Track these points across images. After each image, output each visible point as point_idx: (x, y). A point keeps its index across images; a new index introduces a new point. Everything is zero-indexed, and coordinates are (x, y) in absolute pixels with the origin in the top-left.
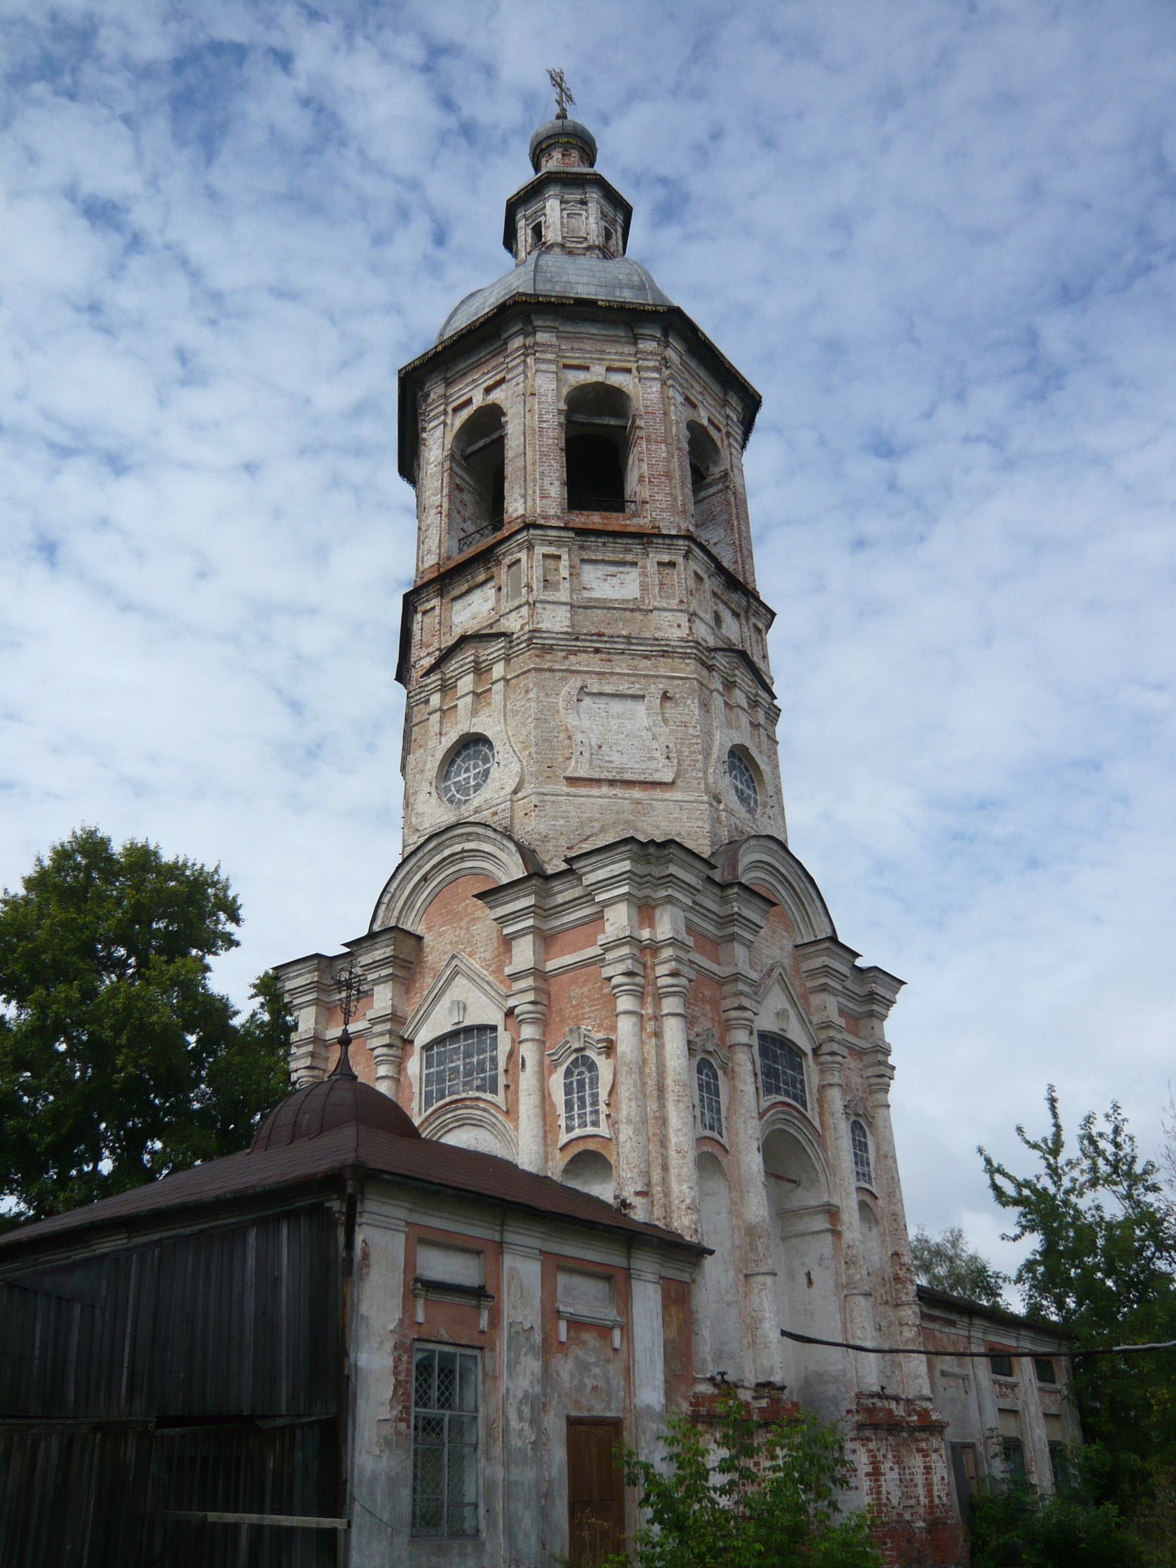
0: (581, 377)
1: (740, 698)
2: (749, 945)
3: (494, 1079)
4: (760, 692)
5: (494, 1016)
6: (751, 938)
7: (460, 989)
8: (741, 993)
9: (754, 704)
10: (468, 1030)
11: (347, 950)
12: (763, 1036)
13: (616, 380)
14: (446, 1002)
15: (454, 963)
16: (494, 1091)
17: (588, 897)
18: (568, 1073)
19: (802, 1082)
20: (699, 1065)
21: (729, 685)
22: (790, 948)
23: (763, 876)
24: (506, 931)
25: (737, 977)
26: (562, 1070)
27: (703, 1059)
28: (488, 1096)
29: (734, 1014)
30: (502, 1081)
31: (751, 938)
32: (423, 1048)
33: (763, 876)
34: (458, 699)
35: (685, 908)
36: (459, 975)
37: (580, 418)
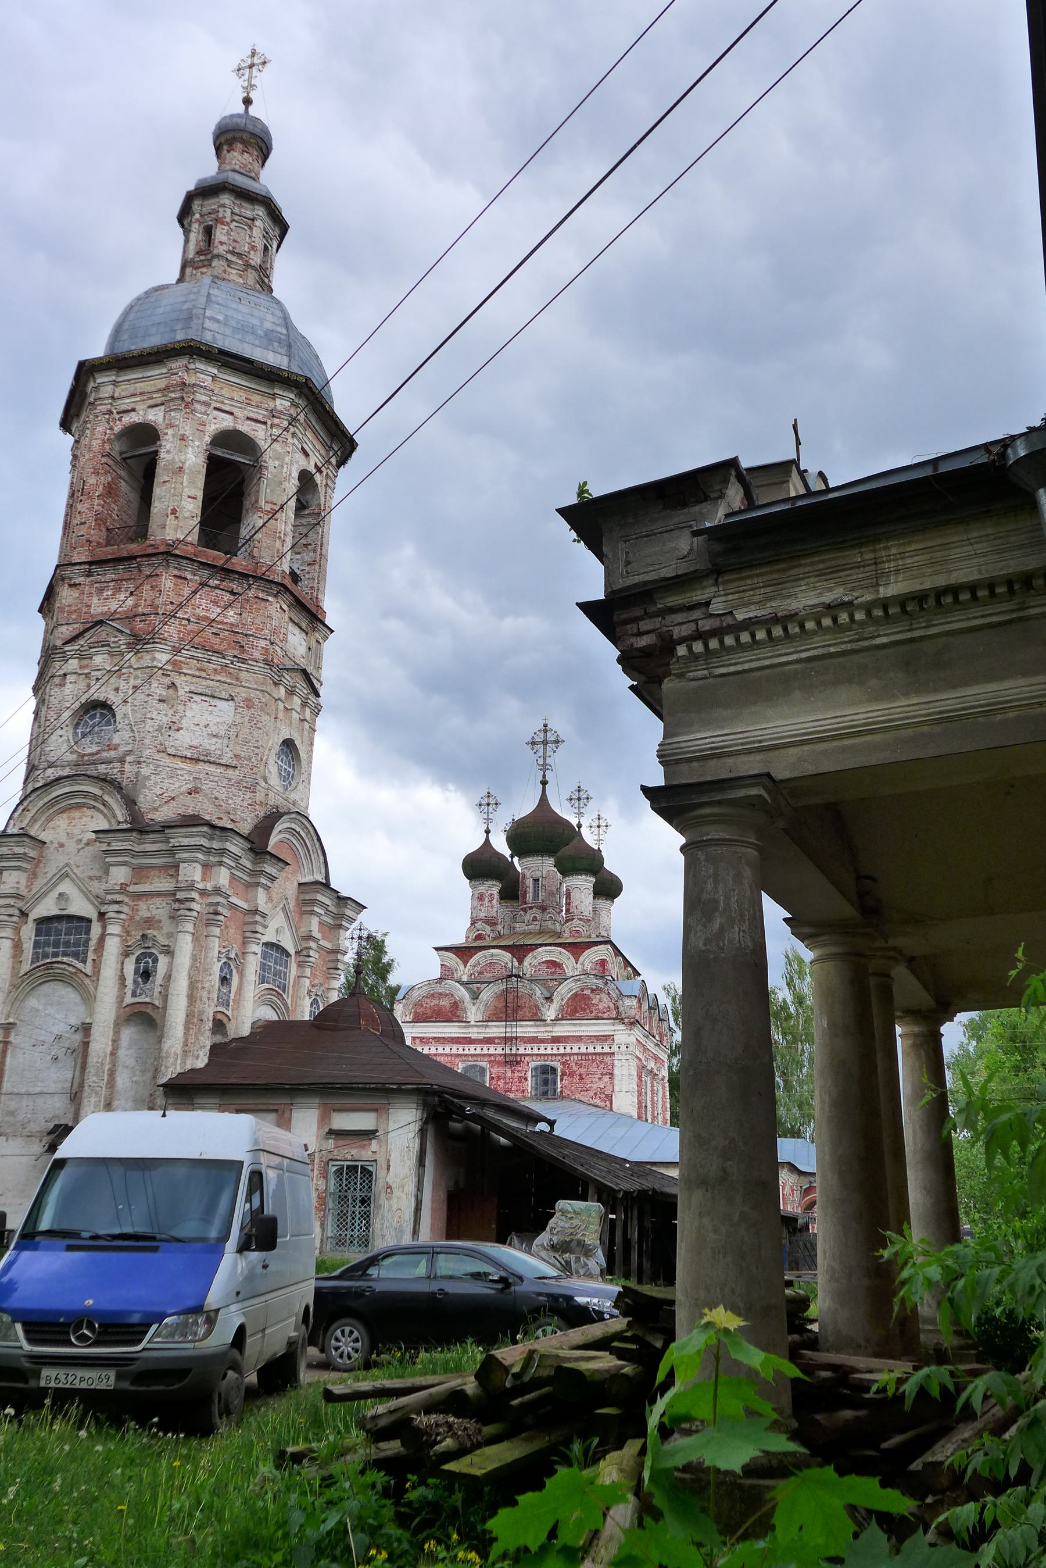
1: (297, 701)
2: (267, 888)
3: (85, 953)
5: (93, 914)
6: (269, 884)
7: (66, 887)
8: (256, 923)
9: (304, 704)
10: (70, 918)
12: (267, 944)
14: (54, 894)
15: (66, 869)
16: (84, 962)
17: (172, 852)
19: (285, 973)
21: (291, 692)
22: (296, 884)
23: (287, 836)
24: (107, 860)
25: (255, 912)
26: (133, 958)
27: (225, 963)
29: (248, 934)
30: (91, 956)
31: (269, 884)
32: (35, 920)
33: (287, 836)
35: (230, 868)
36: (67, 879)
37: (219, 452)
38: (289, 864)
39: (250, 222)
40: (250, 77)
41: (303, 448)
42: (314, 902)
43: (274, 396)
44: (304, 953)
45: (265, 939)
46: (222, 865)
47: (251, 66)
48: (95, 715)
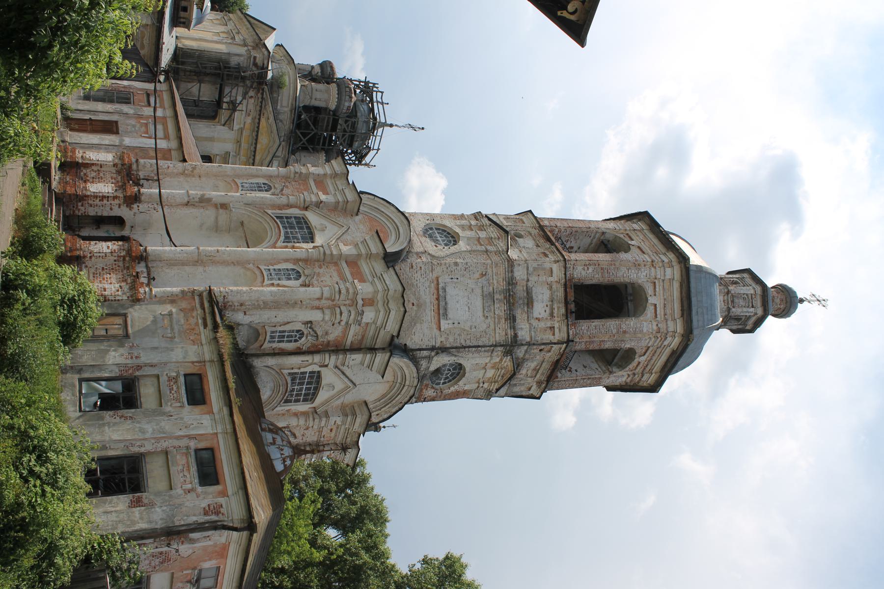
0: (649, 291)
2: (362, 363)
4: (497, 384)
6: (365, 365)
11: (351, 183)
12: (319, 375)
13: (650, 310)
18: (293, 270)
20: (300, 330)
27: (303, 334)
28: (282, 238)
30: (289, 245)
31: (365, 365)
34: (476, 231)
38: (383, 377)
39: (751, 305)
40: (813, 301)
41: (649, 347)
42: (354, 414)
43: (674, 320)
44: (316, 416)
45: (324, 371)
46: (376, 312)
47: (818, 300)
48: (449, 238)
